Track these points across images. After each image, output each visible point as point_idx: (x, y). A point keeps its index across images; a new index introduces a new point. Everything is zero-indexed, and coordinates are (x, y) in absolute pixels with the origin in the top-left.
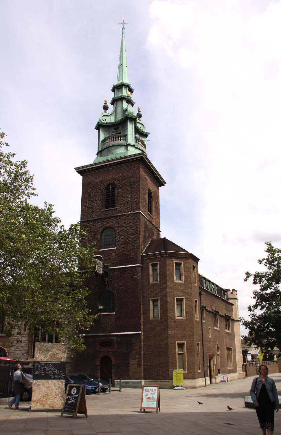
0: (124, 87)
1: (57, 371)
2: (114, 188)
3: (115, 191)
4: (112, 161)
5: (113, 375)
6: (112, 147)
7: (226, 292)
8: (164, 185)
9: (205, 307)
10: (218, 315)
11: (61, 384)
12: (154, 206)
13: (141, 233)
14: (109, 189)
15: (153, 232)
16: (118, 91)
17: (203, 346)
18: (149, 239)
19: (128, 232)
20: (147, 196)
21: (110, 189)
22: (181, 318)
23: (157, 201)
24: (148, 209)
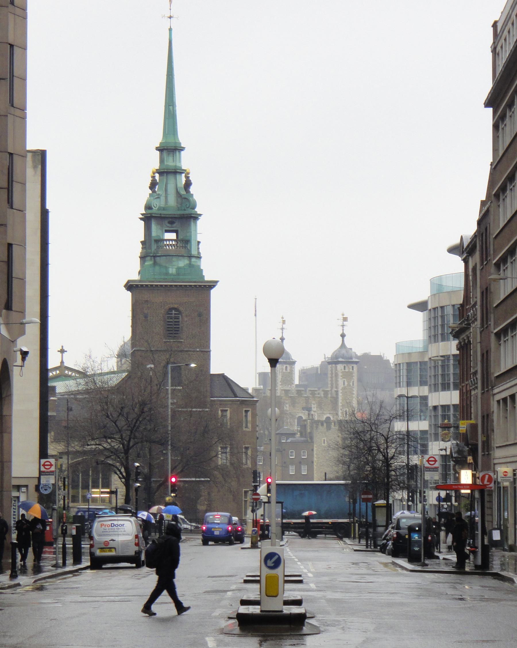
3: (178, 319)
16: (169, 154)
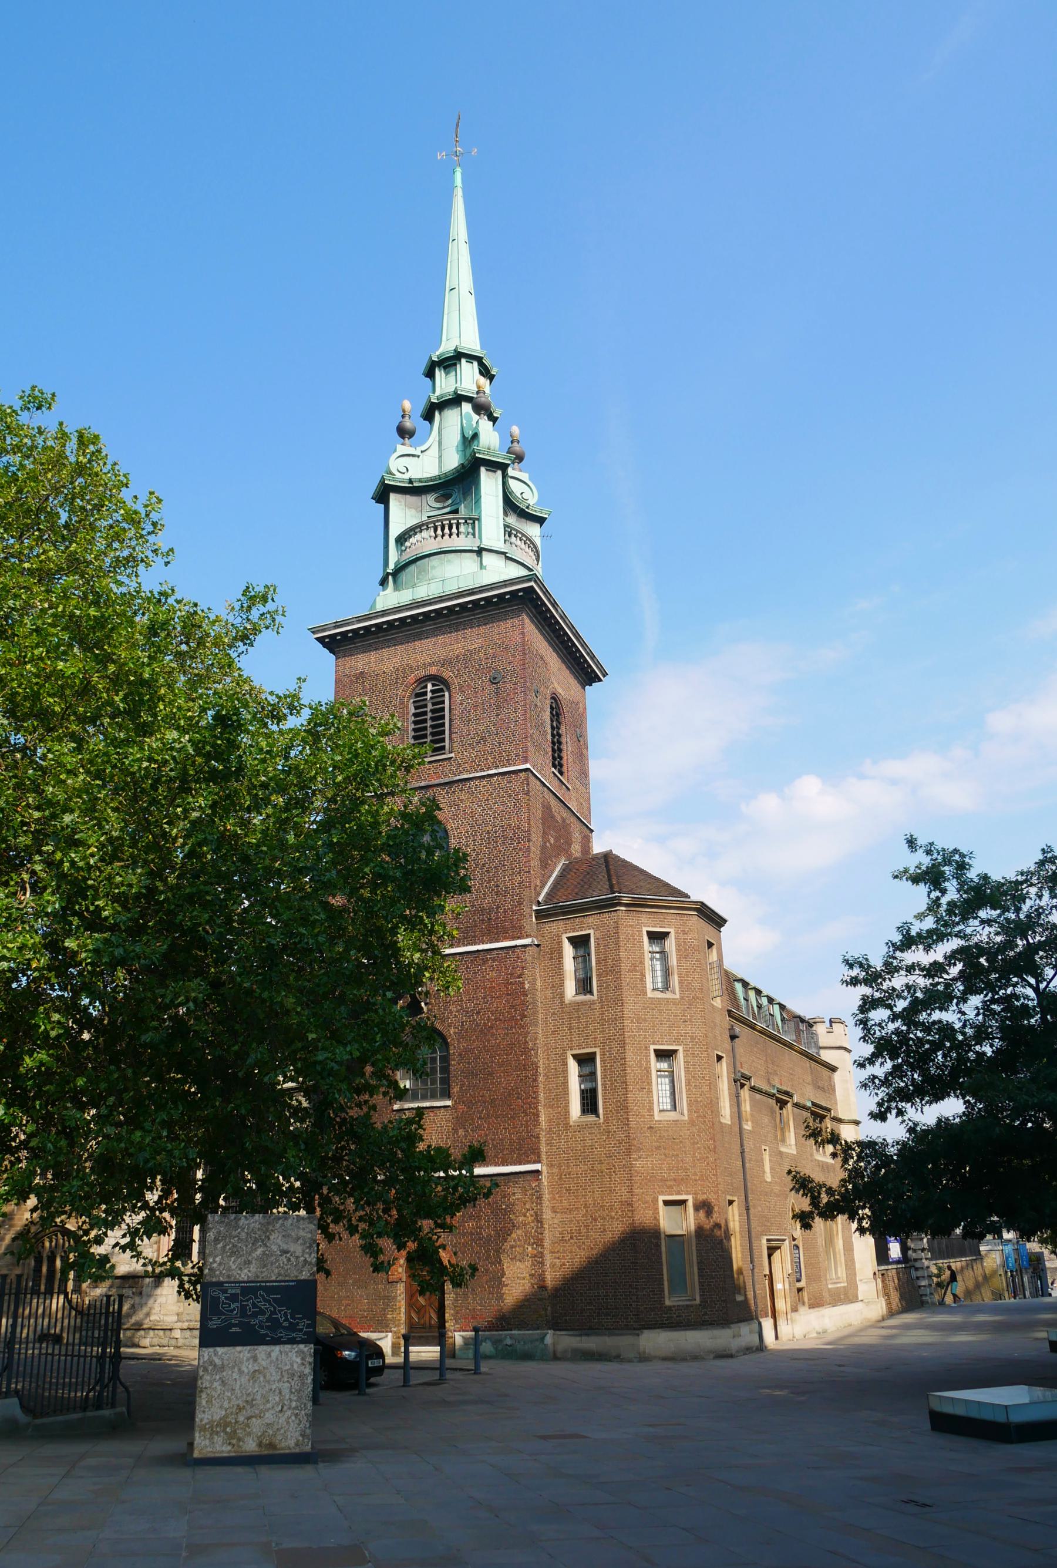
0: (463, 361)
1: (286, 1315)
2: (442, 690)
3: (443, 702)
4: (431, 604)
5: (447, 1315)
6: (432, 558)
7: (811, 1026)
8: (600, 680)
9: (749, 1079)
10: (789, 1105)
11: (299, 1360)
12: (570, 748)
13: (534, 837)
14: (425, 694)
15: (570, 833)
16: (447, 374)
17: (748, 1209)
18: (557, 856)
19: (488, 832)
20: (547, 716)
21: (429, 695)
22: (673, 1116)
23: (578, 733)
24: (554, 758)
